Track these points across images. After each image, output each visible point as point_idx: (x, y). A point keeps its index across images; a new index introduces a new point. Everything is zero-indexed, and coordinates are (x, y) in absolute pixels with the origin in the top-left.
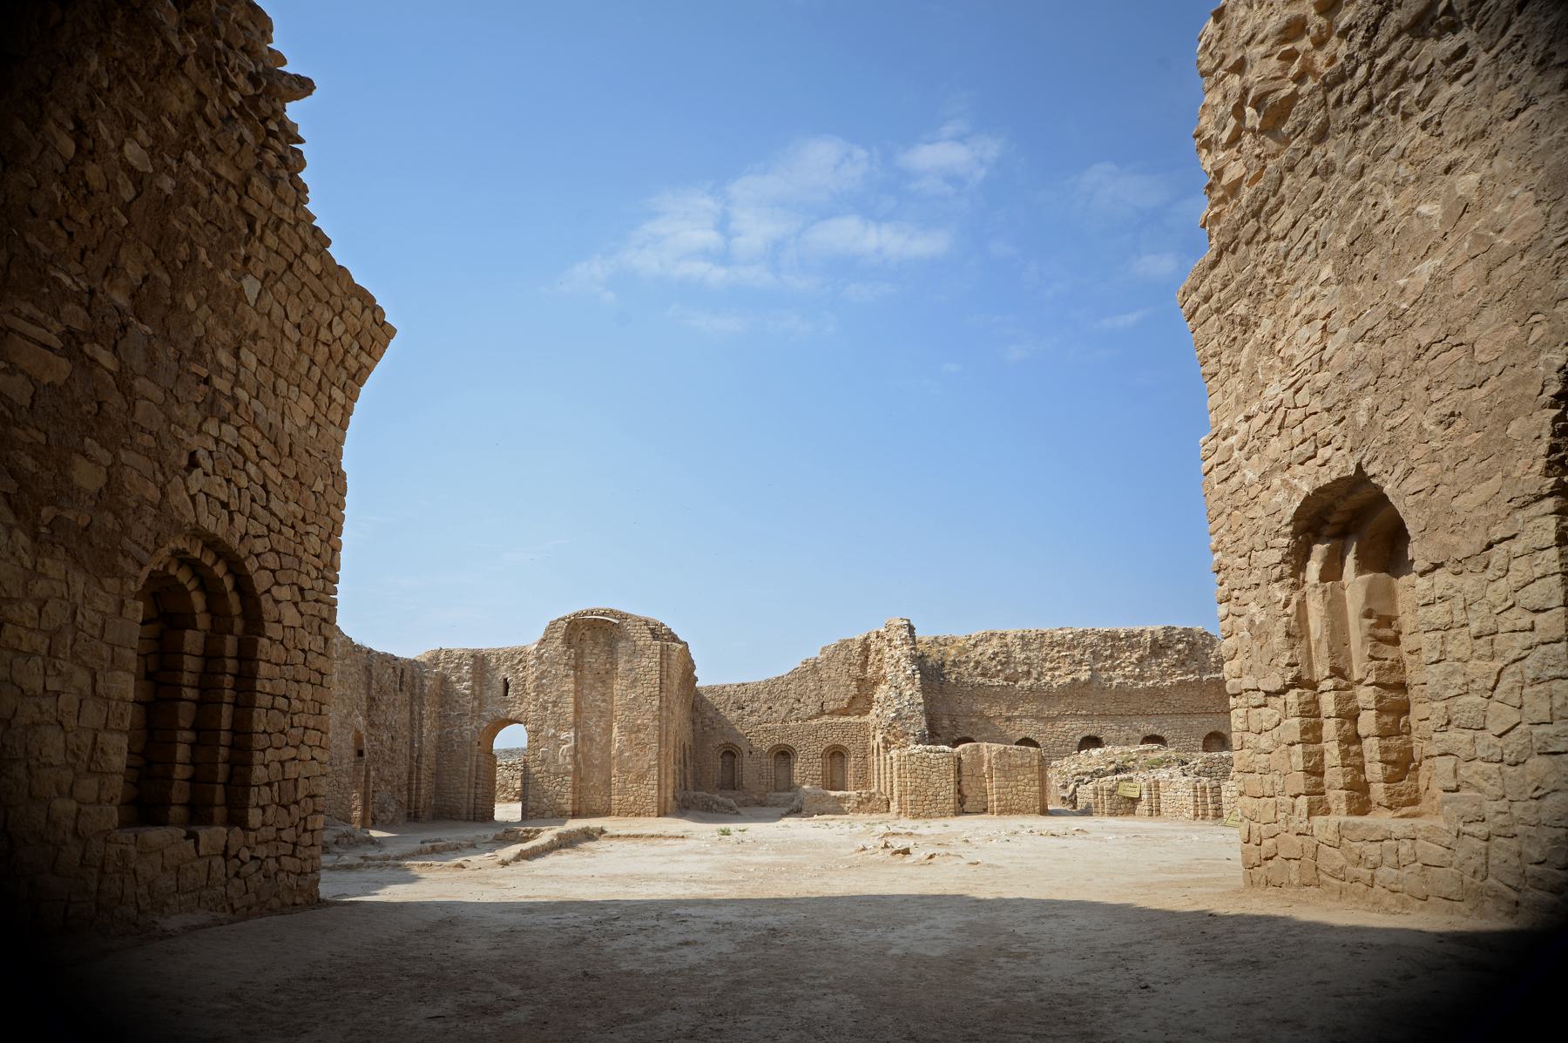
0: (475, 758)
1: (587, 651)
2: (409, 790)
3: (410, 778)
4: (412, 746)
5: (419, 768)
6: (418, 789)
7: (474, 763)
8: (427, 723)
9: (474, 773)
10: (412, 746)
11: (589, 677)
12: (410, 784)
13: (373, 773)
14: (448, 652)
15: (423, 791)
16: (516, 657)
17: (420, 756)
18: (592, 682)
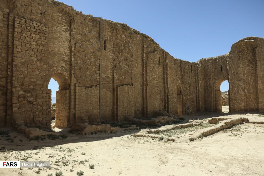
0: (214, 92)
1: (246, 53)
2: (197, 102)
3: (197, 99)
4: (196, 89)
5: (199, 95)
6: (199, 102)
7: (214, 94)
8: (200, 82)
9: (214, 97)
10: (196, 89)
11: (247, 62)
12: (197, 101)
13: (184, 98)
14: (205, 59)
15: (200, 103)
16: (223, 59)
17: (199, 92)
18: (248, 64)
